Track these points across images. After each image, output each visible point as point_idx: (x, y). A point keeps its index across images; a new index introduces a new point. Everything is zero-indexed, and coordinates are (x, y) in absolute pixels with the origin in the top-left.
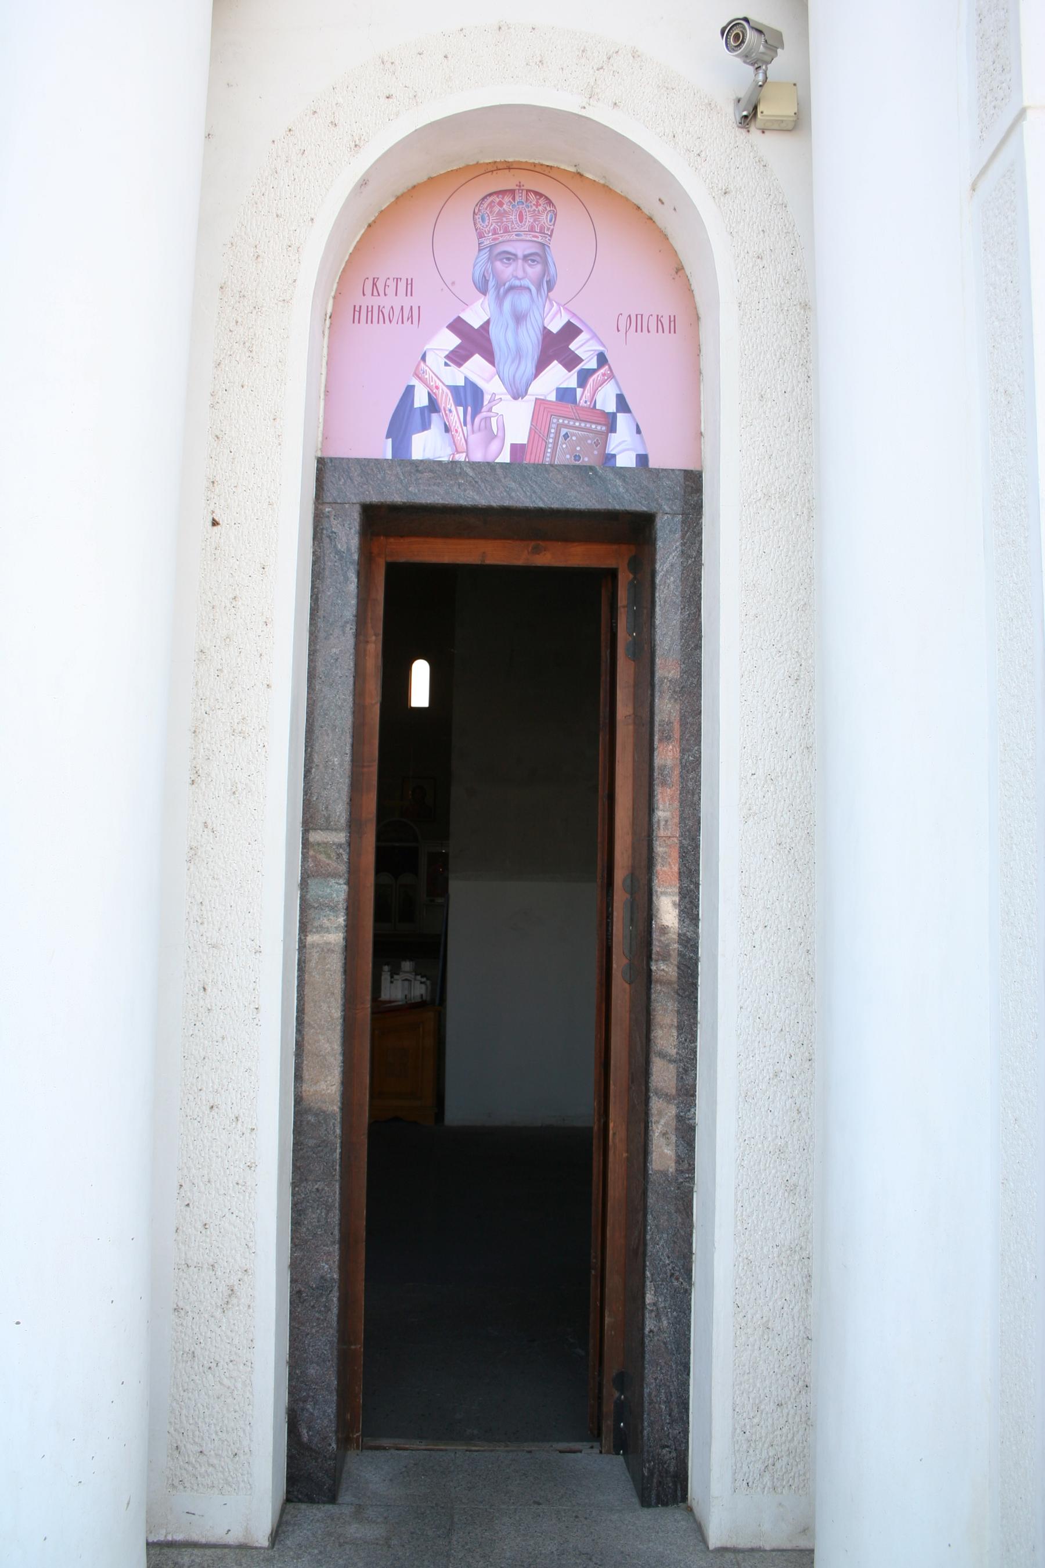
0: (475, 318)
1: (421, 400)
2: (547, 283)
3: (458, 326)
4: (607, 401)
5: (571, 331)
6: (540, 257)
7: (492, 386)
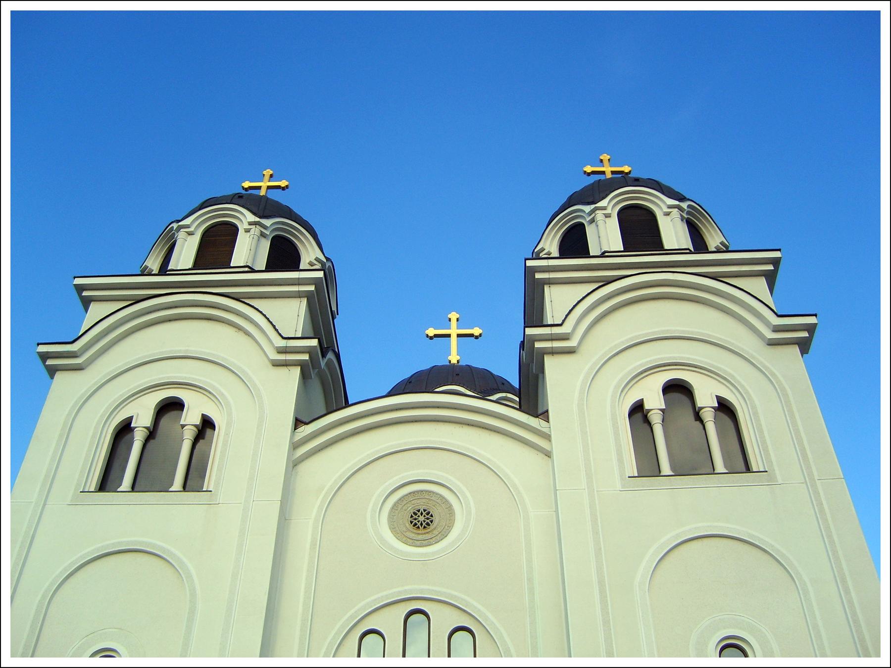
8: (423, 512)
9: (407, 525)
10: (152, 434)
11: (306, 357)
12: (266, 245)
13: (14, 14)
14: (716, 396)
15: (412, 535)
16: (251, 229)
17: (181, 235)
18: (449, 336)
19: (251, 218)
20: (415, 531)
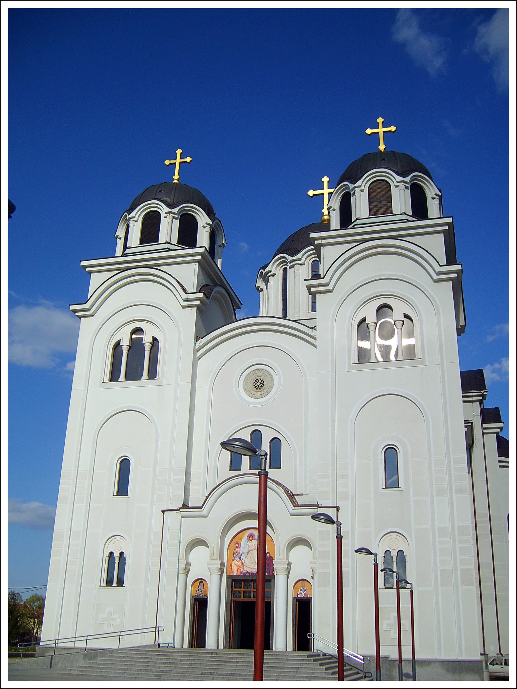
0: (301, 589)
1: (298, 593)
2: (305, 586)
3: (300, 589)
4: (308, 593)
5: (306, 589)
6: (305, 585)
7: (302, 593)
8: (259, 380)
9: (252, 387)
11: (198, 302)
12: (177, 223)
13: (12, 12)
14: (404, 314)
16: (167, 216)
17: (131, 222)
18: (323, 194)
19: (166, 209)
20: (256, 390)
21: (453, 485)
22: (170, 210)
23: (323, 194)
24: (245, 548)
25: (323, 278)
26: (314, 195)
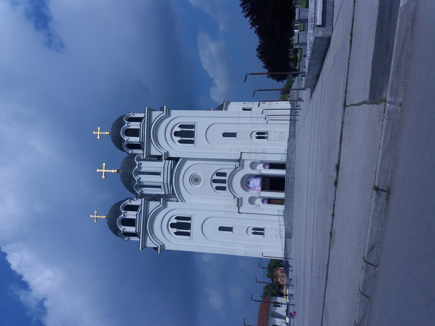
10: (178, 228)
11: (164, 200)
15: (199, 182)
18: (105, 172)
19: (122, 215)
21: (237, 115)
22: (123, 214)
23: (105, 172)
24: (252, 185)
25: (162, 154)
26: (104, 176)
